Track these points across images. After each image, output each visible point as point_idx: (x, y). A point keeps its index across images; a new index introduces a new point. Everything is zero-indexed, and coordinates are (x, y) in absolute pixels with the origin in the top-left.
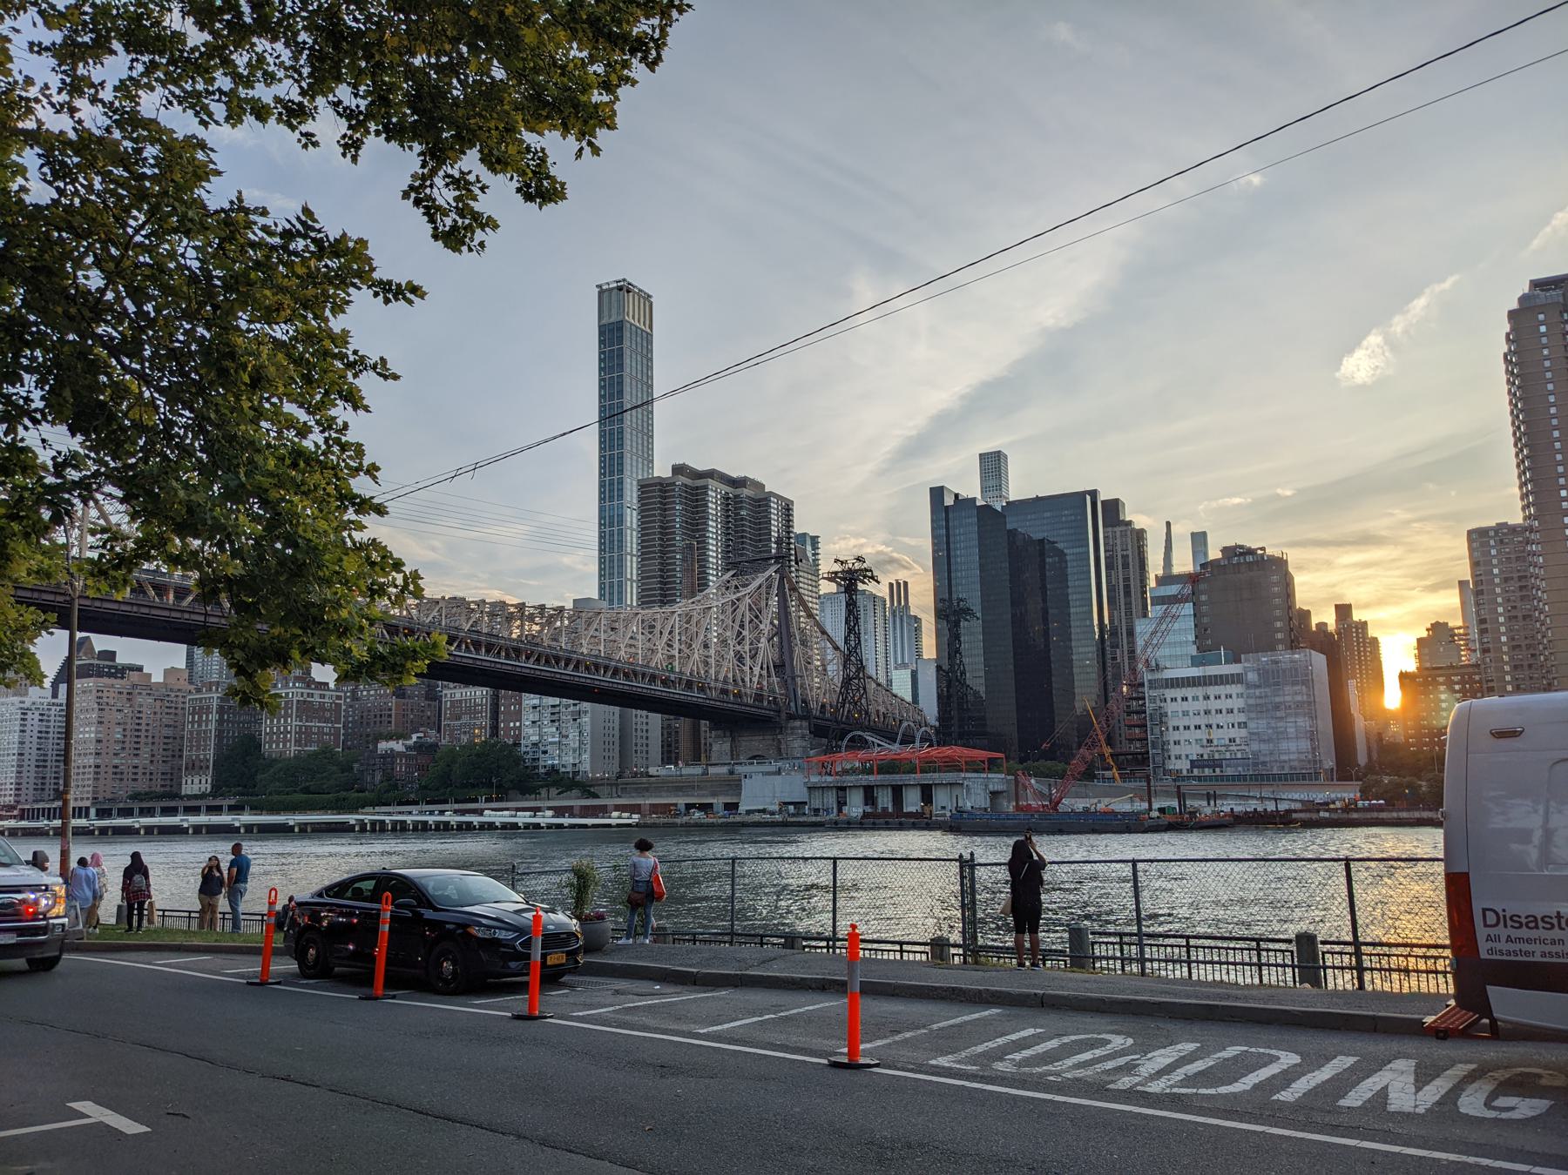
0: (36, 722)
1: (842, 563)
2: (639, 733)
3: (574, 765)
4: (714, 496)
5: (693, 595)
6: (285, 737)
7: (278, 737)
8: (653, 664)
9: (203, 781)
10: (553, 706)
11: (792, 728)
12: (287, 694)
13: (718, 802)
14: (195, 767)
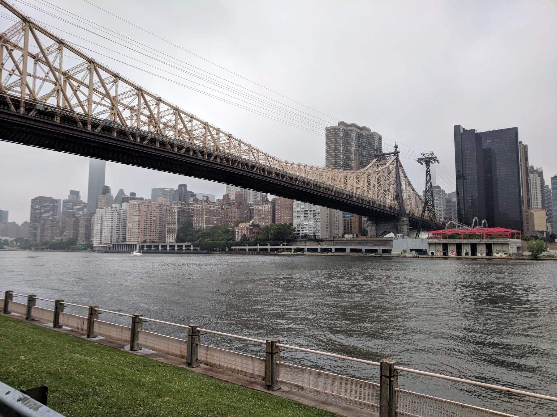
0: (116, 215)
1: (424, 155)
2: (336, 222)
3: (314, 233)
4: (353, 135)
5: (359, 169)
6: (202, 221)
7: (199, 222)
8: (358, 193)
9: (174, 236)
10: (305, 211)
11: (403, 221)
12: (202, 206)
13: (380, 248)
14: (170, 231)
